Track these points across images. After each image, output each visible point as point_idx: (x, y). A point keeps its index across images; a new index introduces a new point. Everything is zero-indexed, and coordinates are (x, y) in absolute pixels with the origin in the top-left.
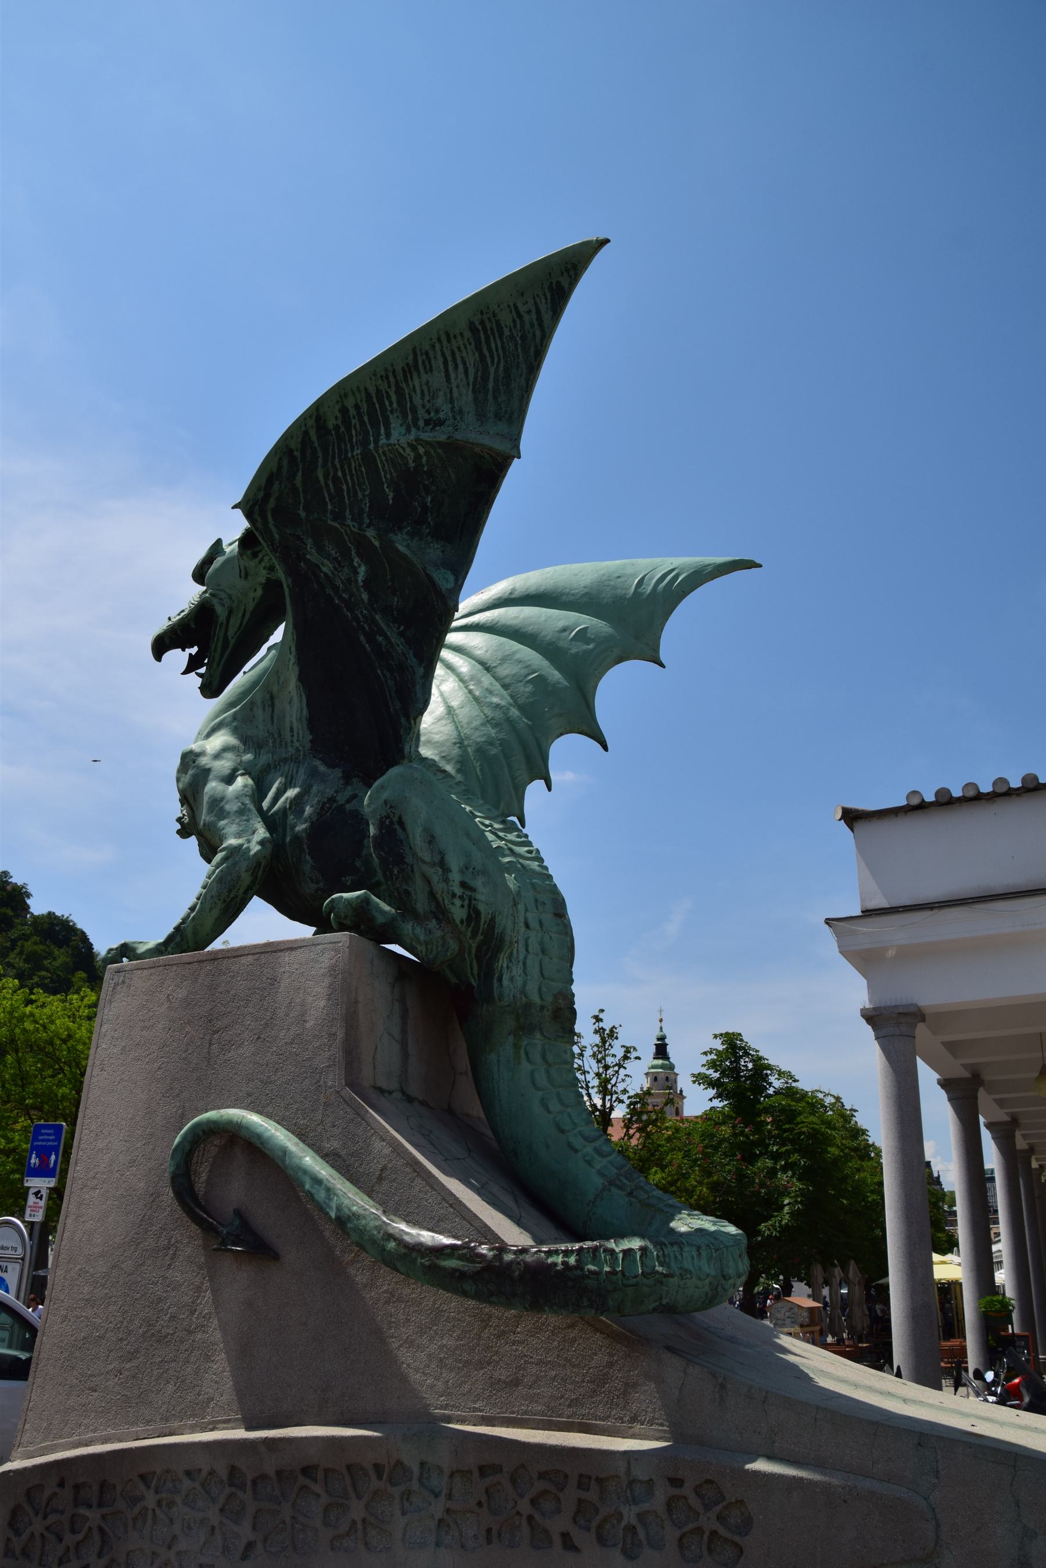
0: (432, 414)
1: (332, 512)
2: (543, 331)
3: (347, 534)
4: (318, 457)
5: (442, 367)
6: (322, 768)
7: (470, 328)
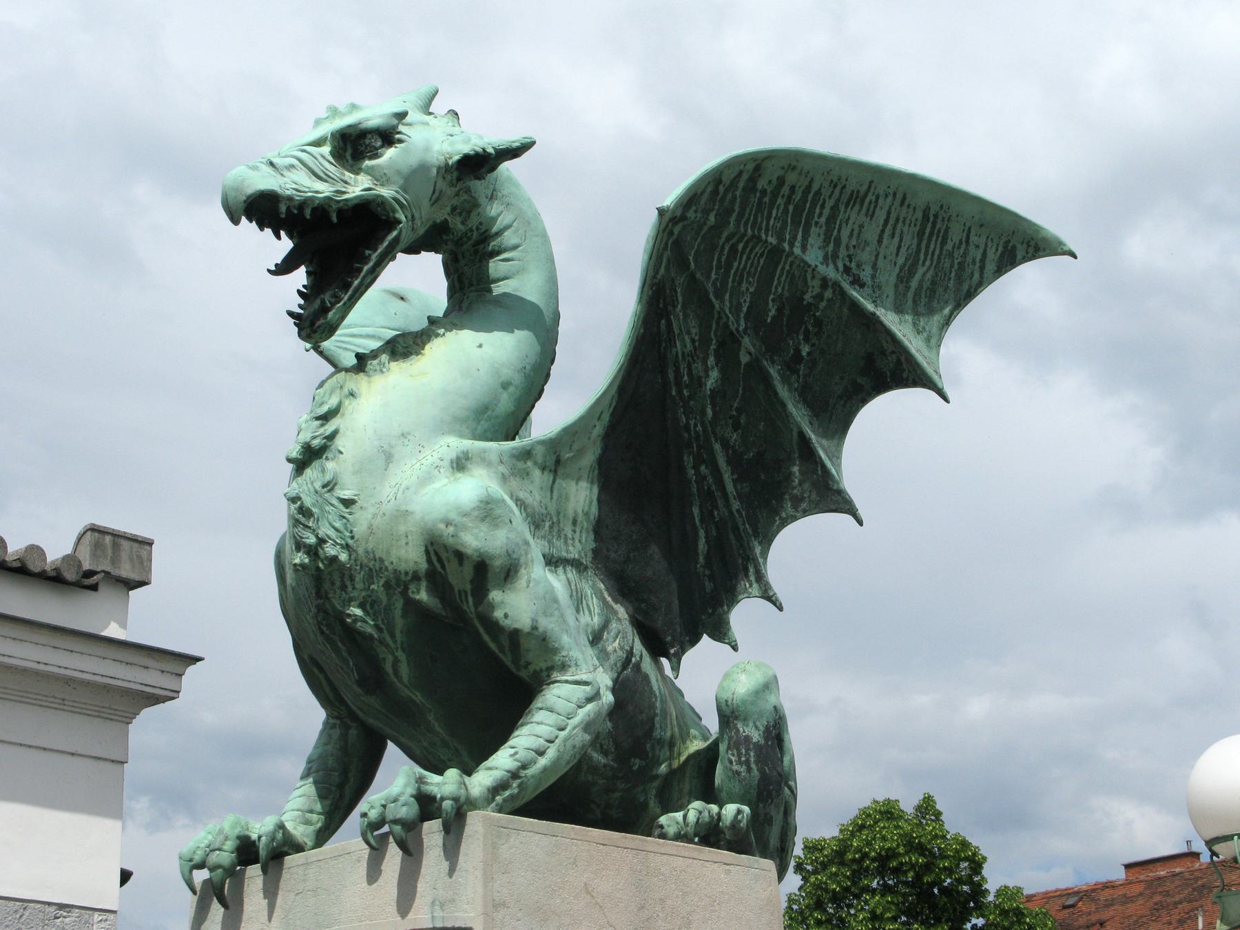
3: (717, 323)
4: (733, 211)
5: (882, 222)
7: (924, 211)
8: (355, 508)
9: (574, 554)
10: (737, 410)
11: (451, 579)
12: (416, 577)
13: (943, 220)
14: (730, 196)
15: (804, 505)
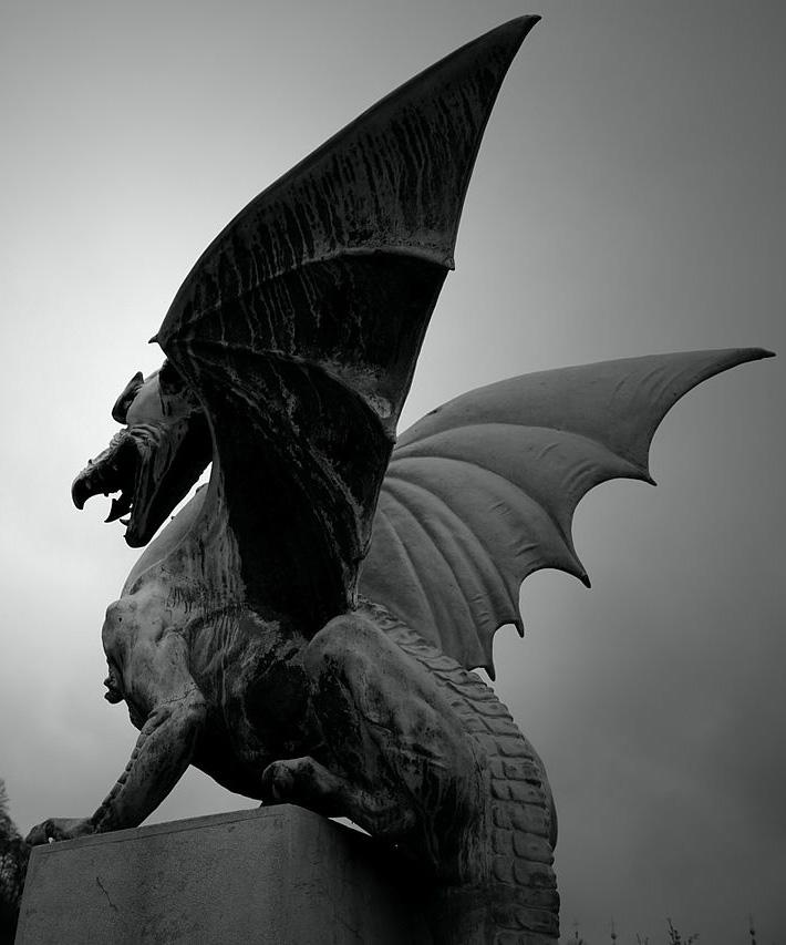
0: (358, 226)
1: (257, 339)
2: (472, 125)
6: (258, 621)
13: (413, 118)
14: (228, 276)
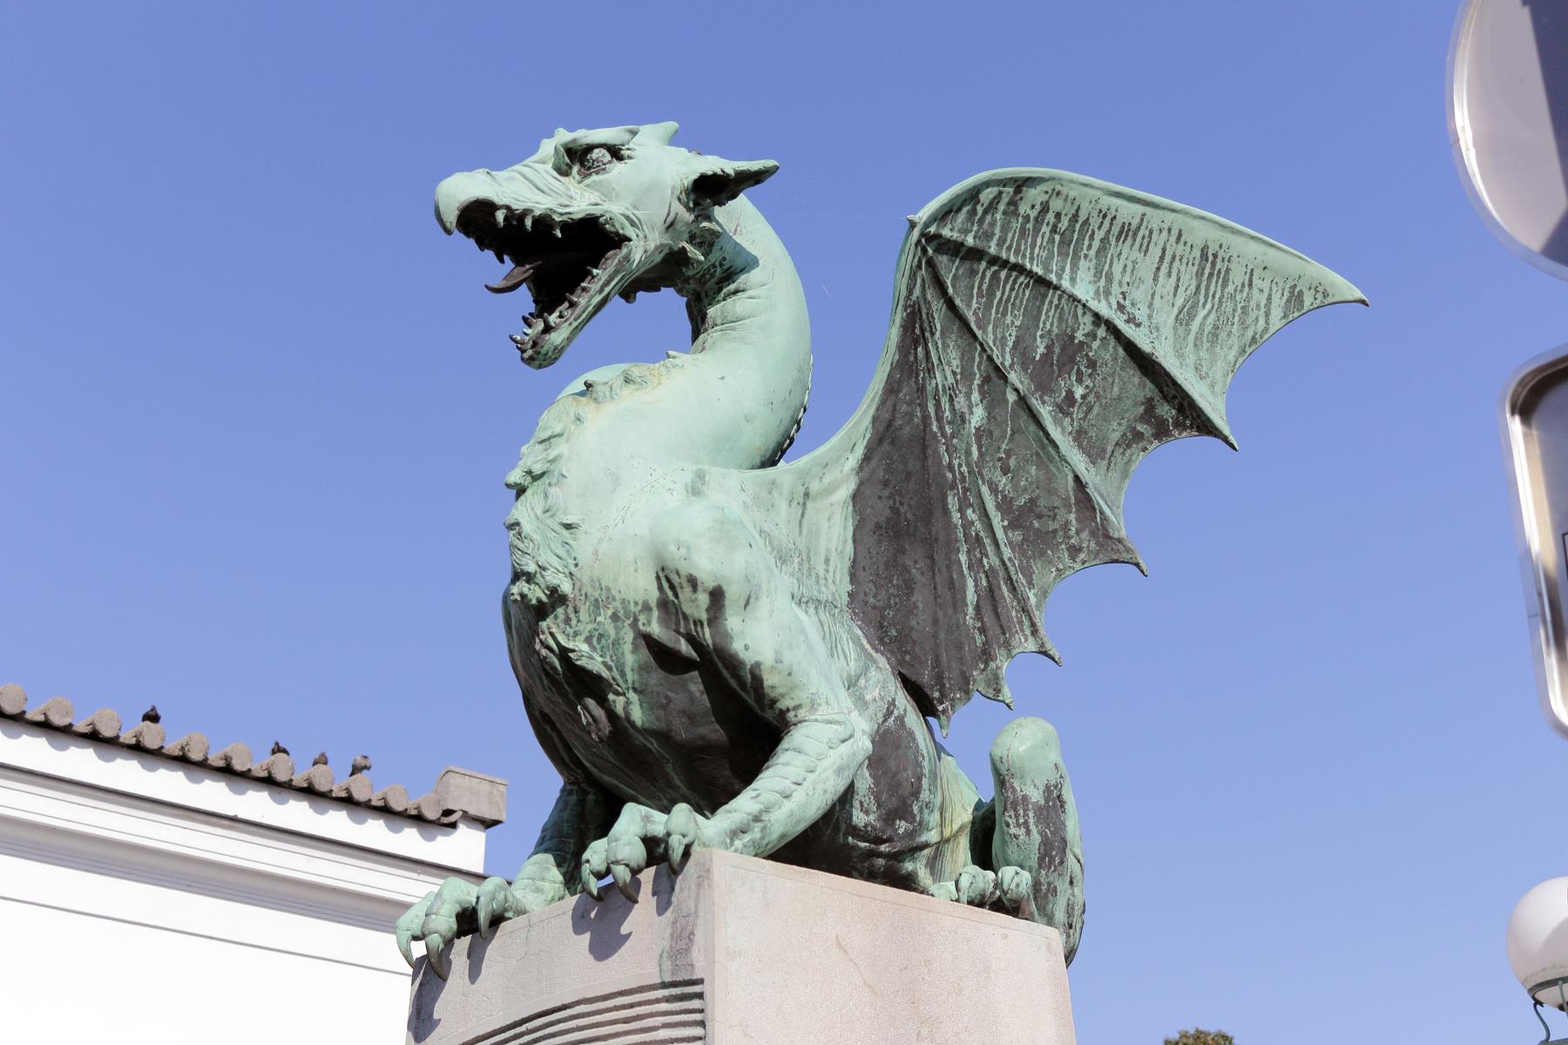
8: (579, 533)
9: (826, 595)
10: (1006, 452)
11: (687, 608)
12: (646, 608)
14: (988, 218)
15: (1082, 556)
